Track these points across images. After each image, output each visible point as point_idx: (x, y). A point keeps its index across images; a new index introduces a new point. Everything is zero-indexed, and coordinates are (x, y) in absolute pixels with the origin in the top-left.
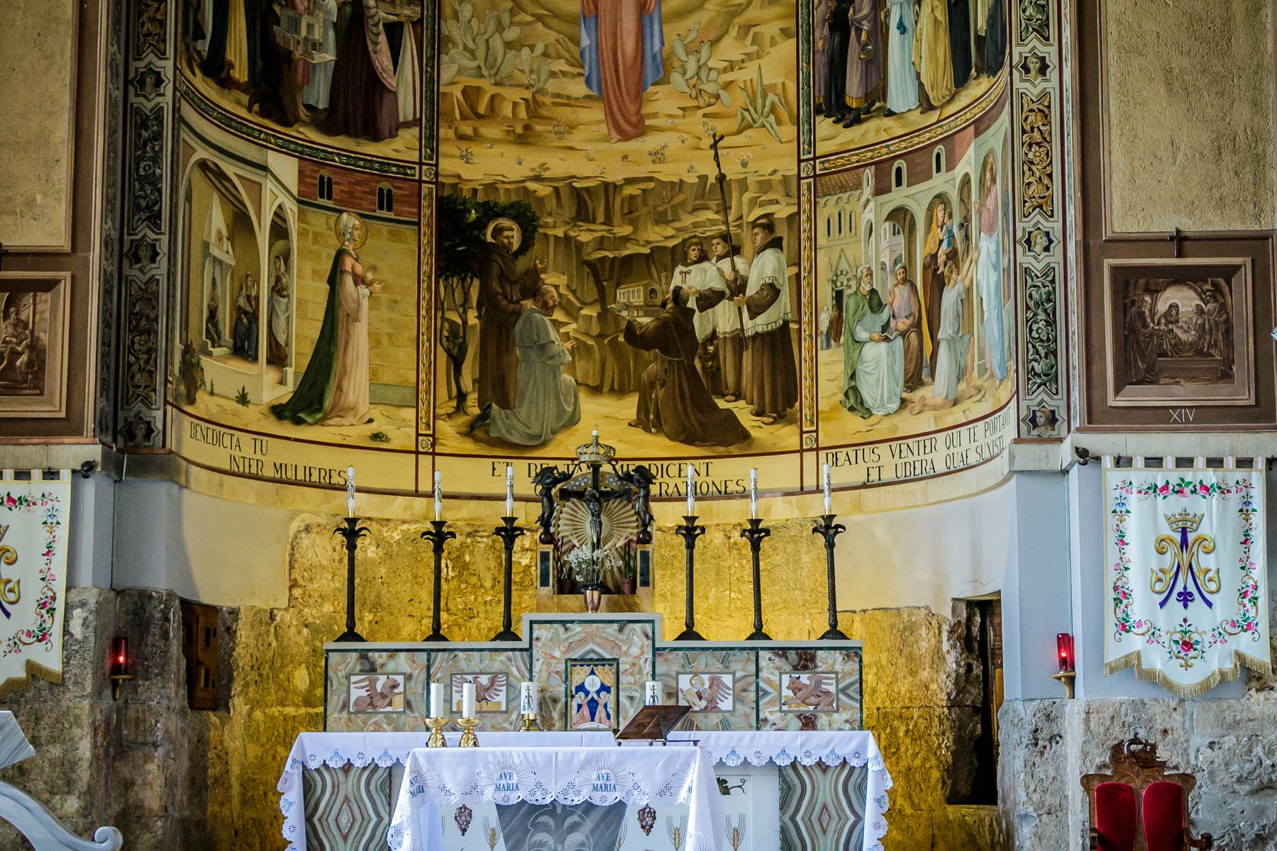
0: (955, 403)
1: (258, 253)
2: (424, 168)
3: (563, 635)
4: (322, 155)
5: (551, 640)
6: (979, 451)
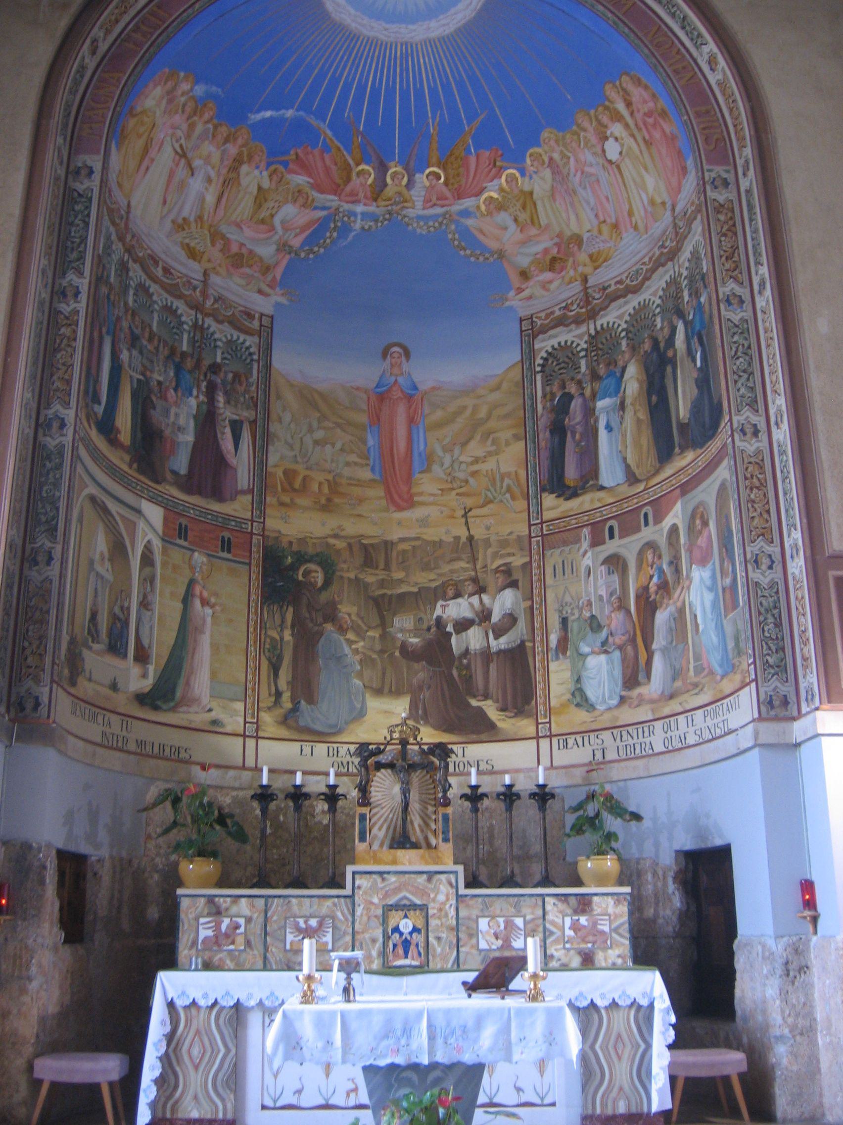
0: (672, 697)
1: (131, 575)
2: (255, 524)
3: (380, 885)
4: (181, 508)
5: (371, 888)
6: (698, 732)
